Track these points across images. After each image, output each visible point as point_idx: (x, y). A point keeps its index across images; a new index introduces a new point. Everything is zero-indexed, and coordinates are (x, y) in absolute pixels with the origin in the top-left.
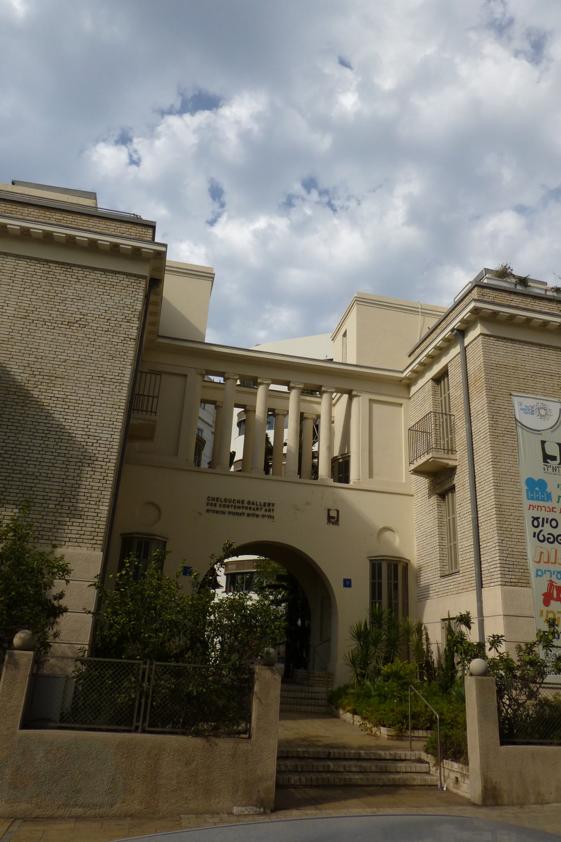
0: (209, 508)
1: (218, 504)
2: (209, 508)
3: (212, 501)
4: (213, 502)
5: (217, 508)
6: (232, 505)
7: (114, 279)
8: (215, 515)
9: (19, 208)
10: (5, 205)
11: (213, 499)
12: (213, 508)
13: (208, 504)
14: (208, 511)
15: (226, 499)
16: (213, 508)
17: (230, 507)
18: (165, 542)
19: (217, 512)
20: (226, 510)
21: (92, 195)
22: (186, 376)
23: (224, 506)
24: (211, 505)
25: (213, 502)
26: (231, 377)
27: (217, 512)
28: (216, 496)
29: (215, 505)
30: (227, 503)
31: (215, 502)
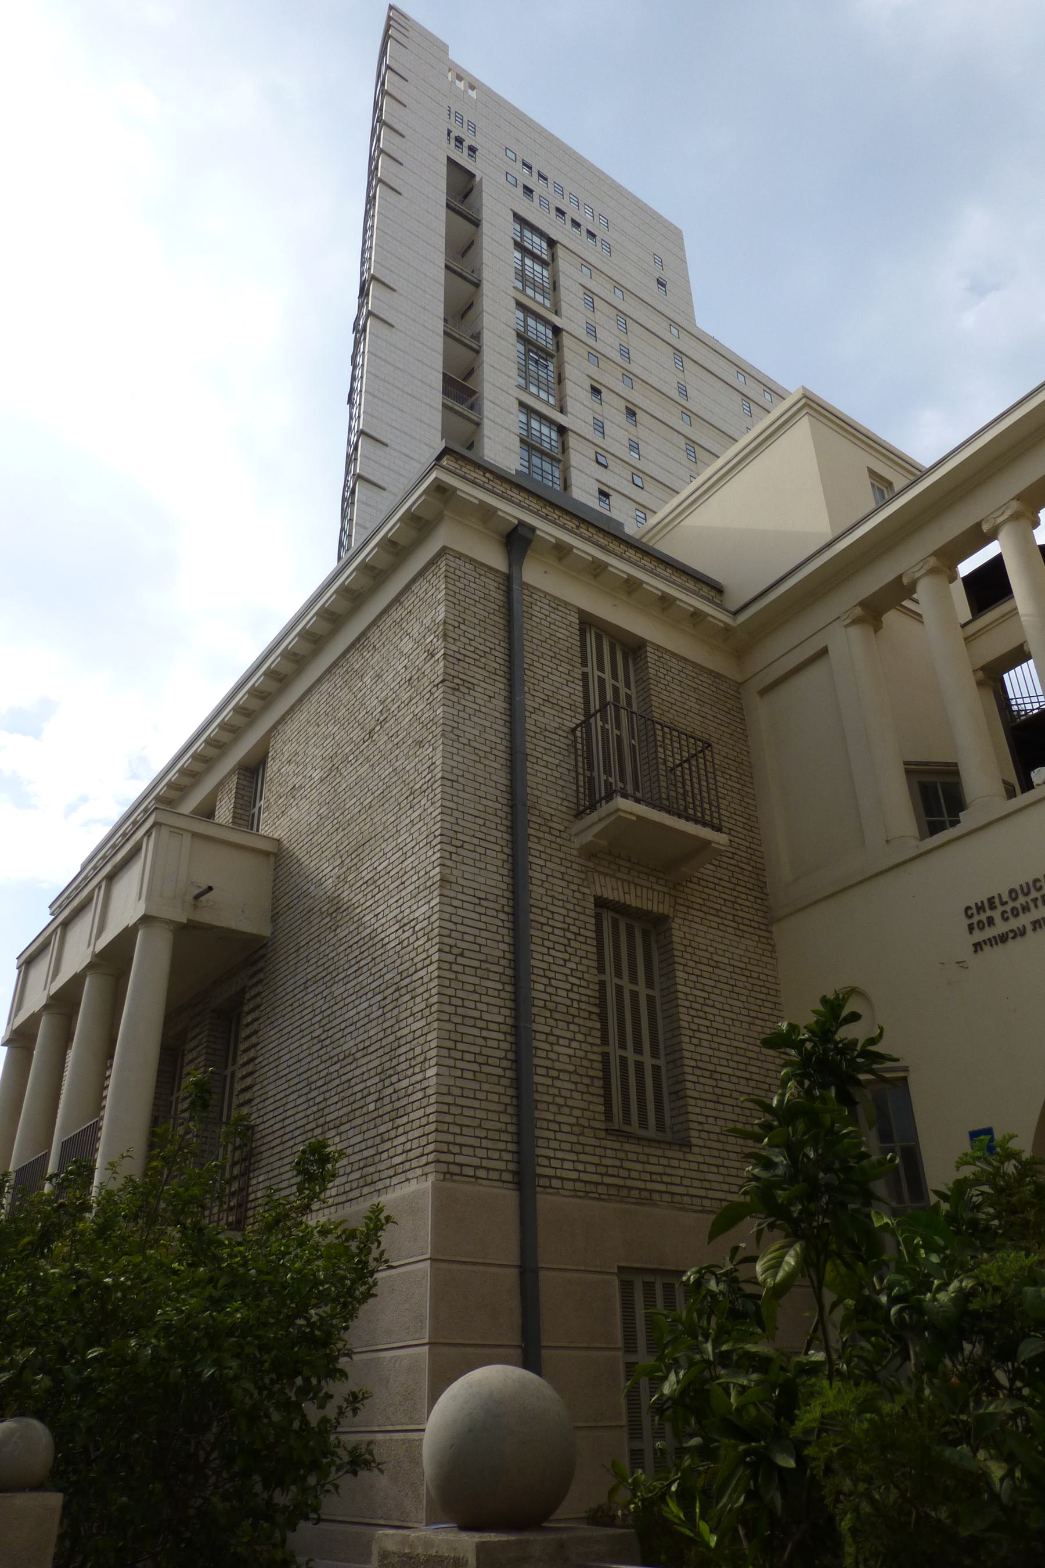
0: (978, 936)
1: (996, 915)
2: (978, 936)
3: (978, 915)
4: (983, 917)
5: (1001, 927)
6: (1035, 900)
7: (410, 601)
8: (1000, 949)
11: (980, 908)
12: (989, 933)
13: (971, 928)
14: (978, 947)
15: (1011, 891)
16: (989, 933)
17: (1032, 905)
18: (905, 1079)
19: (1003, 939)
20: (1025, 920)
22: (824, 652)
23: (1015, 912)
24: (981, 925)
25: (983, 917)
26: (917, 575)
27: (1003, 939)
28: (982, 897)
29: (991, 921)
30: (1022, 900)
31: (989, 913)
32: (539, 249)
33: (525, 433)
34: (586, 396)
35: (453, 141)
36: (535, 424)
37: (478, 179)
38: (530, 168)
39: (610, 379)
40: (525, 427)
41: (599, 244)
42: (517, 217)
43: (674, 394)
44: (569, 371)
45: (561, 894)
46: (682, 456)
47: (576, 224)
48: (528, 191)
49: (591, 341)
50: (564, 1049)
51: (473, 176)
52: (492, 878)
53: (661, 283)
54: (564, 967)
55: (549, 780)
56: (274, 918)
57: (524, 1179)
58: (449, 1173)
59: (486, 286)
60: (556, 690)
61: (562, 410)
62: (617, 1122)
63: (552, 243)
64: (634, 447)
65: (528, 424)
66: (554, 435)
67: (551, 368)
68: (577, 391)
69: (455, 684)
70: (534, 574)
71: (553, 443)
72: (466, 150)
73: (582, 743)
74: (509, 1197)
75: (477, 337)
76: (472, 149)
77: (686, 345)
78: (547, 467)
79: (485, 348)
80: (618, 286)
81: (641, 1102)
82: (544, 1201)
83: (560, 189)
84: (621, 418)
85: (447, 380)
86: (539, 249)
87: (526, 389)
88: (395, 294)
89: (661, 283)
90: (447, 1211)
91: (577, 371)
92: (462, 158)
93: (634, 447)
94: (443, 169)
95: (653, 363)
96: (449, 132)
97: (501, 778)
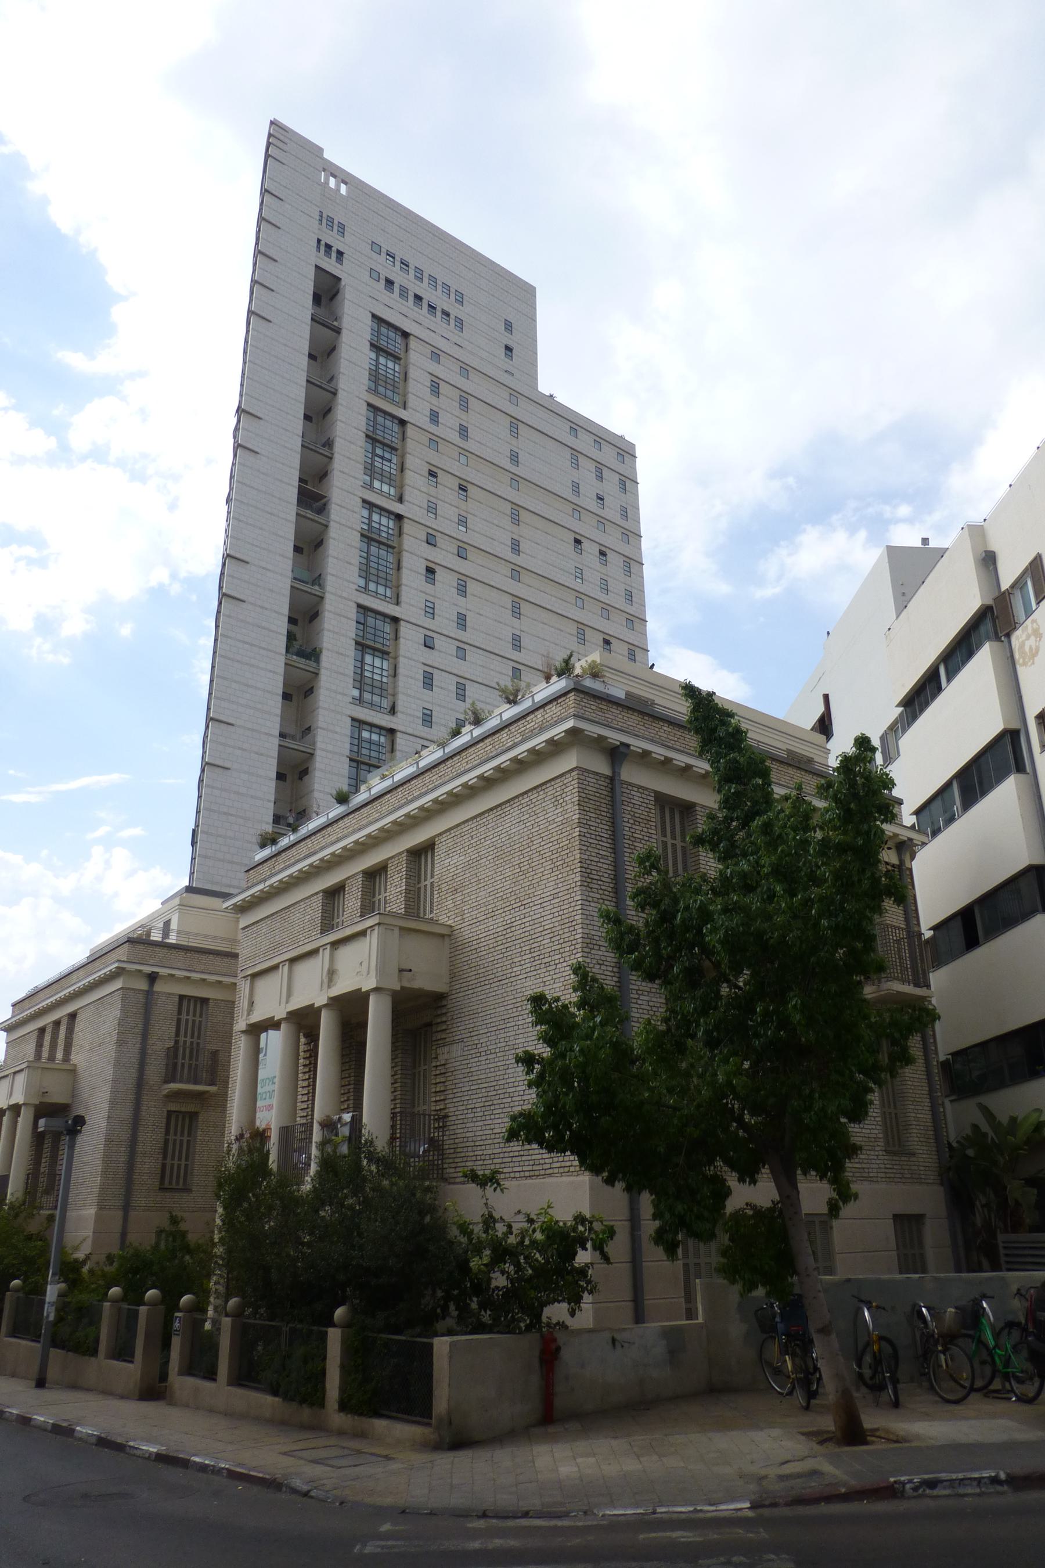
33: (366, 527)
35: (322, 248)
36: (375, 517)
37: (343, 283)
38: (394, 258)
40: (367, 521)
41: (452, 322)
43: (506, 463)
44: (410, 461)
45: (154, 1112)
46: (506, 522)
47: (432, 308)
48: (389, 283)
49: (432, 428)
50: (148, 1166)
51: (340, 279)
52: (127, 1113)
53: (508, 349)
54: (151, 1137)
55: (155, 1070)
56: (73, 1096)
57: (126, 1208)
58: (101, 1207)
59: (341, 394)
60: (163, 1034)
61: (401, 500)
62: (166, 1185)
63: (406, 335)
64: (463, 521)
66: (391, 524)
67: (394, 461)
68: (415, 480)
69: (121, 1043)
70: (158, 987)
71: (391, 532)
73: (173, 1053)
74: (120, 1214)
75: (329, 444)
76: (340, 254)
77: (523, 411)
78: (383, 553)
79: (336, 456)
81: (172, 1179)
82: (133, 1214)
83: (419, 275)
87: (371, 487)
88: (262, 422)
89: (508, 349)
90: (98, 1218)
91: (418, 456)
92: (330, 265)
93: (463, 521)
94: (311, 272)
95: (490, 437)
96: (319, 241)
97: (135, 1075)
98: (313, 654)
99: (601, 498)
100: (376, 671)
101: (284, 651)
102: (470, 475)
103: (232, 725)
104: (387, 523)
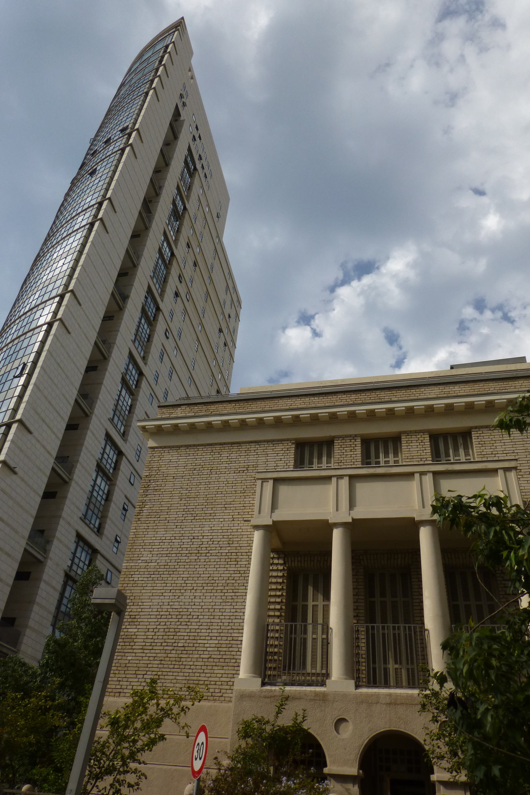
9: (510, 383)
10: (497, 384)
21: (523, 360)
32: (191, 167)
34: (185, 245)
36: (165, 244)
37: (182, 118)
39: (194, 244)
42: (189, 150)
46: (203, 296)
63: (195, 169)
65: (163, 242)
66: (169, 254)
68: (182, 242)
72: (182, 102)
75: (161, 188)
76: (184, 104)
78: (163, 267)
80: (208, 205)
84: (191, 264)
85: (145, 199)
86: (191, 167)
98: (125, 298)
99: (229, 316)
100: (144, 330)
101: (114, 281)
102: (199, 261)
103: (80, 305)
104: (167, 253)
